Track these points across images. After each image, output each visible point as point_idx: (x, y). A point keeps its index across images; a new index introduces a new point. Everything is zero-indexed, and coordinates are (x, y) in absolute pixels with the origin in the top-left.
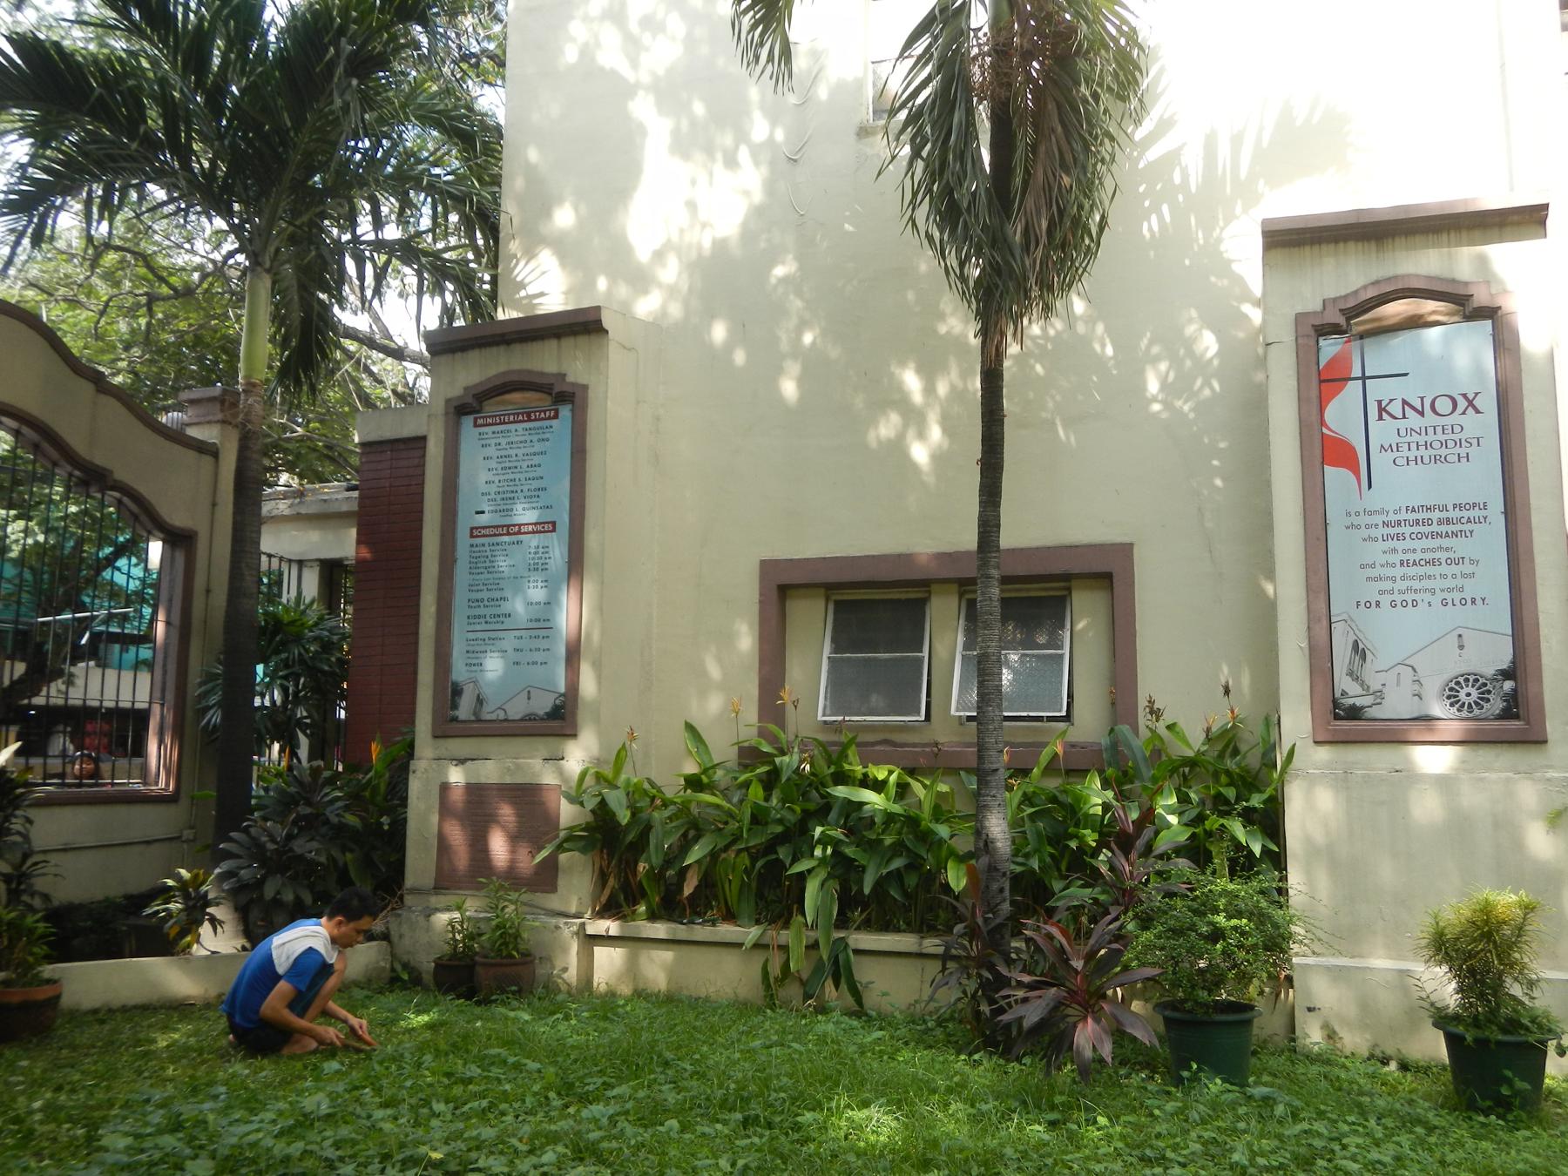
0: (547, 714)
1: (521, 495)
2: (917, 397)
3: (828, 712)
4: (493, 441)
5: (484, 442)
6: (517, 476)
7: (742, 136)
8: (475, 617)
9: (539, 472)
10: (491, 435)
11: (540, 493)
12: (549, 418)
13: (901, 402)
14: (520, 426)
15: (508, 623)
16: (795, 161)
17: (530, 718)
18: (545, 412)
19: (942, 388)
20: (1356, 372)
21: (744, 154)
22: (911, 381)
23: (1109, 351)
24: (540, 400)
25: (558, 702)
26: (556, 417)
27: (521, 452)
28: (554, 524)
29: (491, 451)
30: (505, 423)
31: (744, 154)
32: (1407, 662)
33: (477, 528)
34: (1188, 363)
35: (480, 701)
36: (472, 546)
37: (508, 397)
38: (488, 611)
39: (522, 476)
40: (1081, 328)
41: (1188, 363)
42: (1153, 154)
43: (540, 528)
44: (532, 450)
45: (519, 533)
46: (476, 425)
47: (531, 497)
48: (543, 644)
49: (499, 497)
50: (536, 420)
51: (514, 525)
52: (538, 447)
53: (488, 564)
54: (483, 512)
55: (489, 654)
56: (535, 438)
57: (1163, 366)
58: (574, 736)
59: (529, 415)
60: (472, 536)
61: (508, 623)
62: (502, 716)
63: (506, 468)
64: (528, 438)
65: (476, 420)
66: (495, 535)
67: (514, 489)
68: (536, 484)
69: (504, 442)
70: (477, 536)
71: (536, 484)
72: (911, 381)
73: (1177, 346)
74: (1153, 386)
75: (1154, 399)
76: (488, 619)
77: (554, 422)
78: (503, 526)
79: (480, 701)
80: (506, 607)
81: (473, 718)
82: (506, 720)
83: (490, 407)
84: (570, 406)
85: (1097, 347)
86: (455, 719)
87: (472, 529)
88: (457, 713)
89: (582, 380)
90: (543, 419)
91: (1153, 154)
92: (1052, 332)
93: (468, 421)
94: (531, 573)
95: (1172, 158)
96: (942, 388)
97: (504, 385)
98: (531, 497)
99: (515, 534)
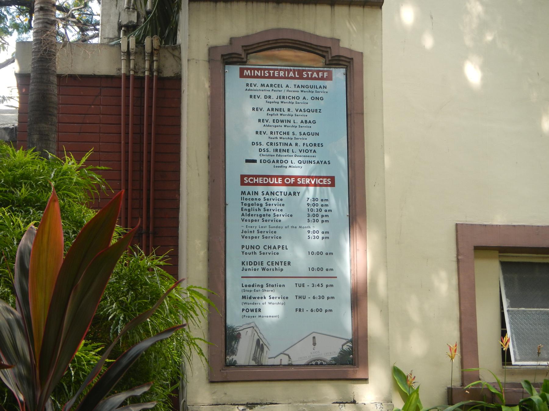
0: (334, 359)
1: (296, 149)
3: (518, 358)
4: (262, 94)
5: (253, 93)
6: (291, 130)
8: (250, 263)
9: (314, 128)
10: (259, 88)
11: (316, 148)
12: (322, 79)
14: (292, 83)
15: (287, 271)
17: (317, 363)
18: (313, 72)
24: (313, 60)
25: (345, 348)
26: (329, 78)
27: (293, 107)
28: (333, 179)
29: (261, 103)
30: (273, 77)
32: (286, 352)
33: (248, 176)
35: (260, 346)
36: (243, 193)
37: (276, 52)
38: (265, 259)
39: (297, 131)
43: (318, 181)
44: (307, 107)
45: (295, 184)
46: (242, 76)
47: (307, 151)
48: (327, 292)
49: (271, 148)
50: (307, 78)
51: (290, 177)
52: (312, 105)
53: (262, 212)
54: (254, 161)
55: (267, 300)
56: (308, 96)
58: (365, 380)
59: (300, 73)
60: (243, 183)
61: (287, 271)
62: (285, 361)
63: (278, 121)
64: (301, 95)
65: (242, 71)
66: (268, 184)
67: (289, 141)
68: (310, 140)
69: (274, 95)
70: (248, 184)
71: (310, 140)
76: (265, 265)
77: (327, 83)
78: (277, 177)
79: (260, 346)
80: (285, 255)
81: (253, 363)
82: (290, 365)
83: (255, 61)
84: (343, 70)
86: (233, 364)
87: (242, 177)
88: (234, 358)
89: (357, 47)
90: (315, 79)
93: (233, 71)
94: (311, 224)
97: (276, 41)
98: (307, 151)
99: (290, 185)
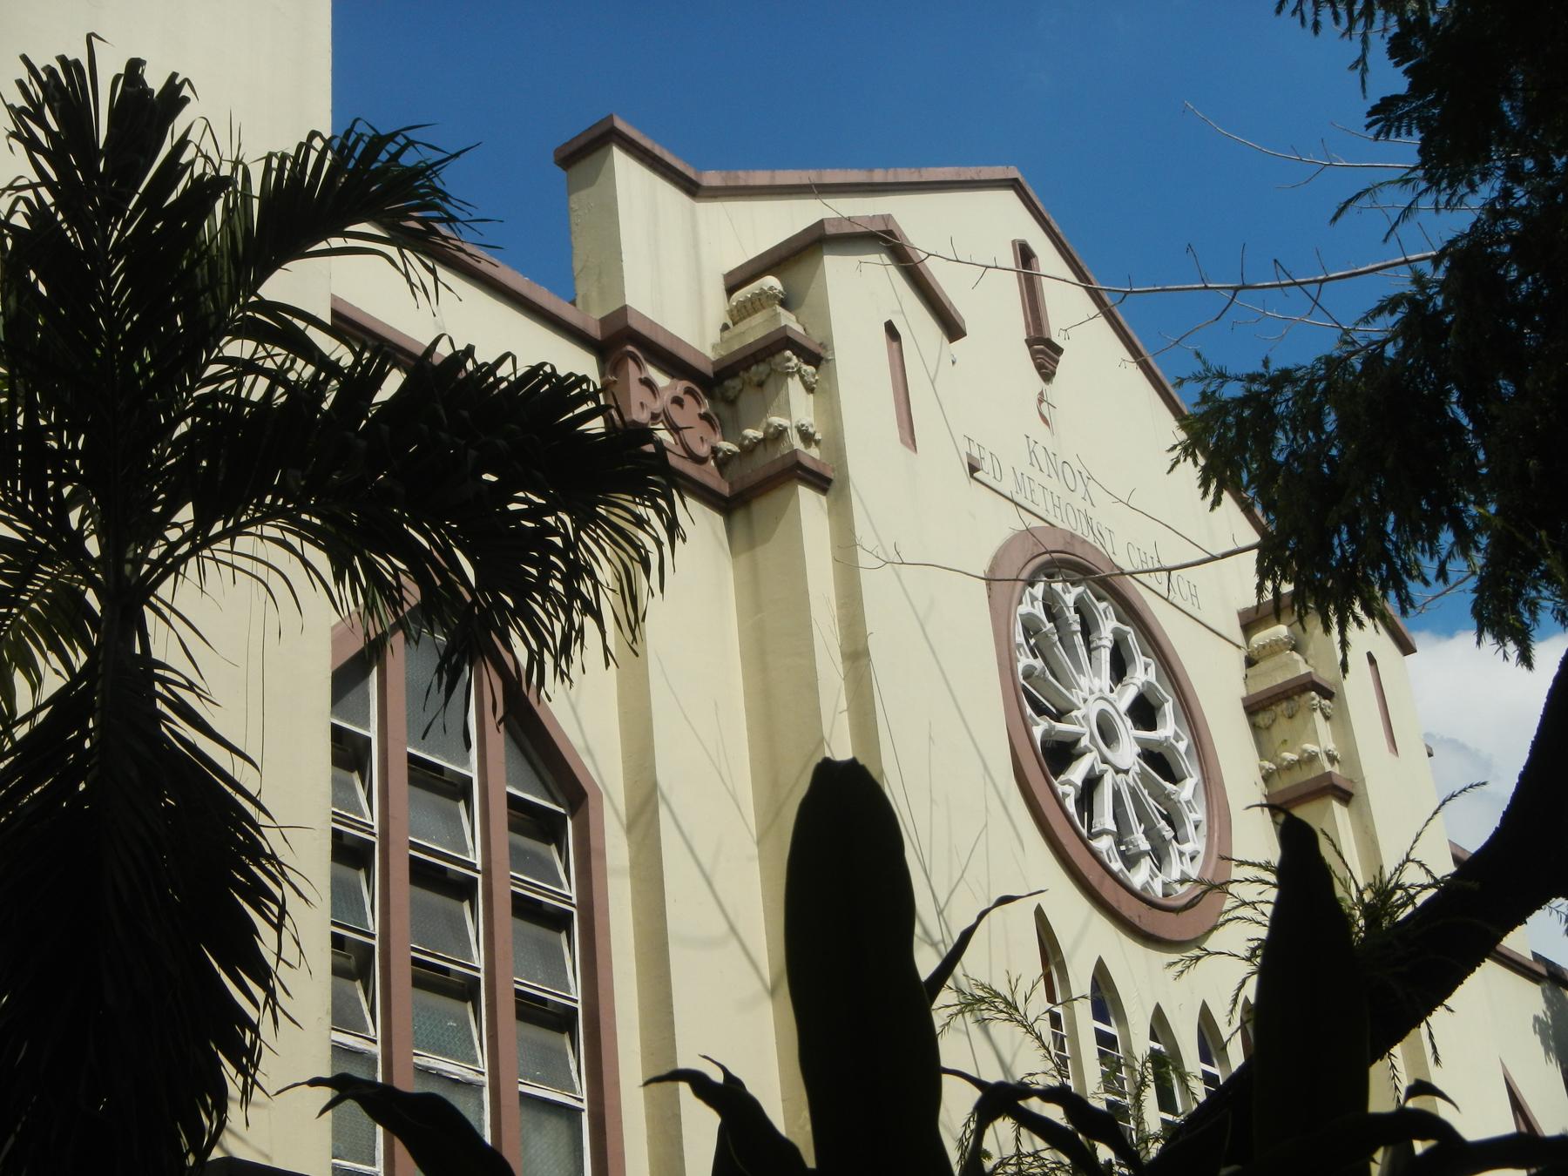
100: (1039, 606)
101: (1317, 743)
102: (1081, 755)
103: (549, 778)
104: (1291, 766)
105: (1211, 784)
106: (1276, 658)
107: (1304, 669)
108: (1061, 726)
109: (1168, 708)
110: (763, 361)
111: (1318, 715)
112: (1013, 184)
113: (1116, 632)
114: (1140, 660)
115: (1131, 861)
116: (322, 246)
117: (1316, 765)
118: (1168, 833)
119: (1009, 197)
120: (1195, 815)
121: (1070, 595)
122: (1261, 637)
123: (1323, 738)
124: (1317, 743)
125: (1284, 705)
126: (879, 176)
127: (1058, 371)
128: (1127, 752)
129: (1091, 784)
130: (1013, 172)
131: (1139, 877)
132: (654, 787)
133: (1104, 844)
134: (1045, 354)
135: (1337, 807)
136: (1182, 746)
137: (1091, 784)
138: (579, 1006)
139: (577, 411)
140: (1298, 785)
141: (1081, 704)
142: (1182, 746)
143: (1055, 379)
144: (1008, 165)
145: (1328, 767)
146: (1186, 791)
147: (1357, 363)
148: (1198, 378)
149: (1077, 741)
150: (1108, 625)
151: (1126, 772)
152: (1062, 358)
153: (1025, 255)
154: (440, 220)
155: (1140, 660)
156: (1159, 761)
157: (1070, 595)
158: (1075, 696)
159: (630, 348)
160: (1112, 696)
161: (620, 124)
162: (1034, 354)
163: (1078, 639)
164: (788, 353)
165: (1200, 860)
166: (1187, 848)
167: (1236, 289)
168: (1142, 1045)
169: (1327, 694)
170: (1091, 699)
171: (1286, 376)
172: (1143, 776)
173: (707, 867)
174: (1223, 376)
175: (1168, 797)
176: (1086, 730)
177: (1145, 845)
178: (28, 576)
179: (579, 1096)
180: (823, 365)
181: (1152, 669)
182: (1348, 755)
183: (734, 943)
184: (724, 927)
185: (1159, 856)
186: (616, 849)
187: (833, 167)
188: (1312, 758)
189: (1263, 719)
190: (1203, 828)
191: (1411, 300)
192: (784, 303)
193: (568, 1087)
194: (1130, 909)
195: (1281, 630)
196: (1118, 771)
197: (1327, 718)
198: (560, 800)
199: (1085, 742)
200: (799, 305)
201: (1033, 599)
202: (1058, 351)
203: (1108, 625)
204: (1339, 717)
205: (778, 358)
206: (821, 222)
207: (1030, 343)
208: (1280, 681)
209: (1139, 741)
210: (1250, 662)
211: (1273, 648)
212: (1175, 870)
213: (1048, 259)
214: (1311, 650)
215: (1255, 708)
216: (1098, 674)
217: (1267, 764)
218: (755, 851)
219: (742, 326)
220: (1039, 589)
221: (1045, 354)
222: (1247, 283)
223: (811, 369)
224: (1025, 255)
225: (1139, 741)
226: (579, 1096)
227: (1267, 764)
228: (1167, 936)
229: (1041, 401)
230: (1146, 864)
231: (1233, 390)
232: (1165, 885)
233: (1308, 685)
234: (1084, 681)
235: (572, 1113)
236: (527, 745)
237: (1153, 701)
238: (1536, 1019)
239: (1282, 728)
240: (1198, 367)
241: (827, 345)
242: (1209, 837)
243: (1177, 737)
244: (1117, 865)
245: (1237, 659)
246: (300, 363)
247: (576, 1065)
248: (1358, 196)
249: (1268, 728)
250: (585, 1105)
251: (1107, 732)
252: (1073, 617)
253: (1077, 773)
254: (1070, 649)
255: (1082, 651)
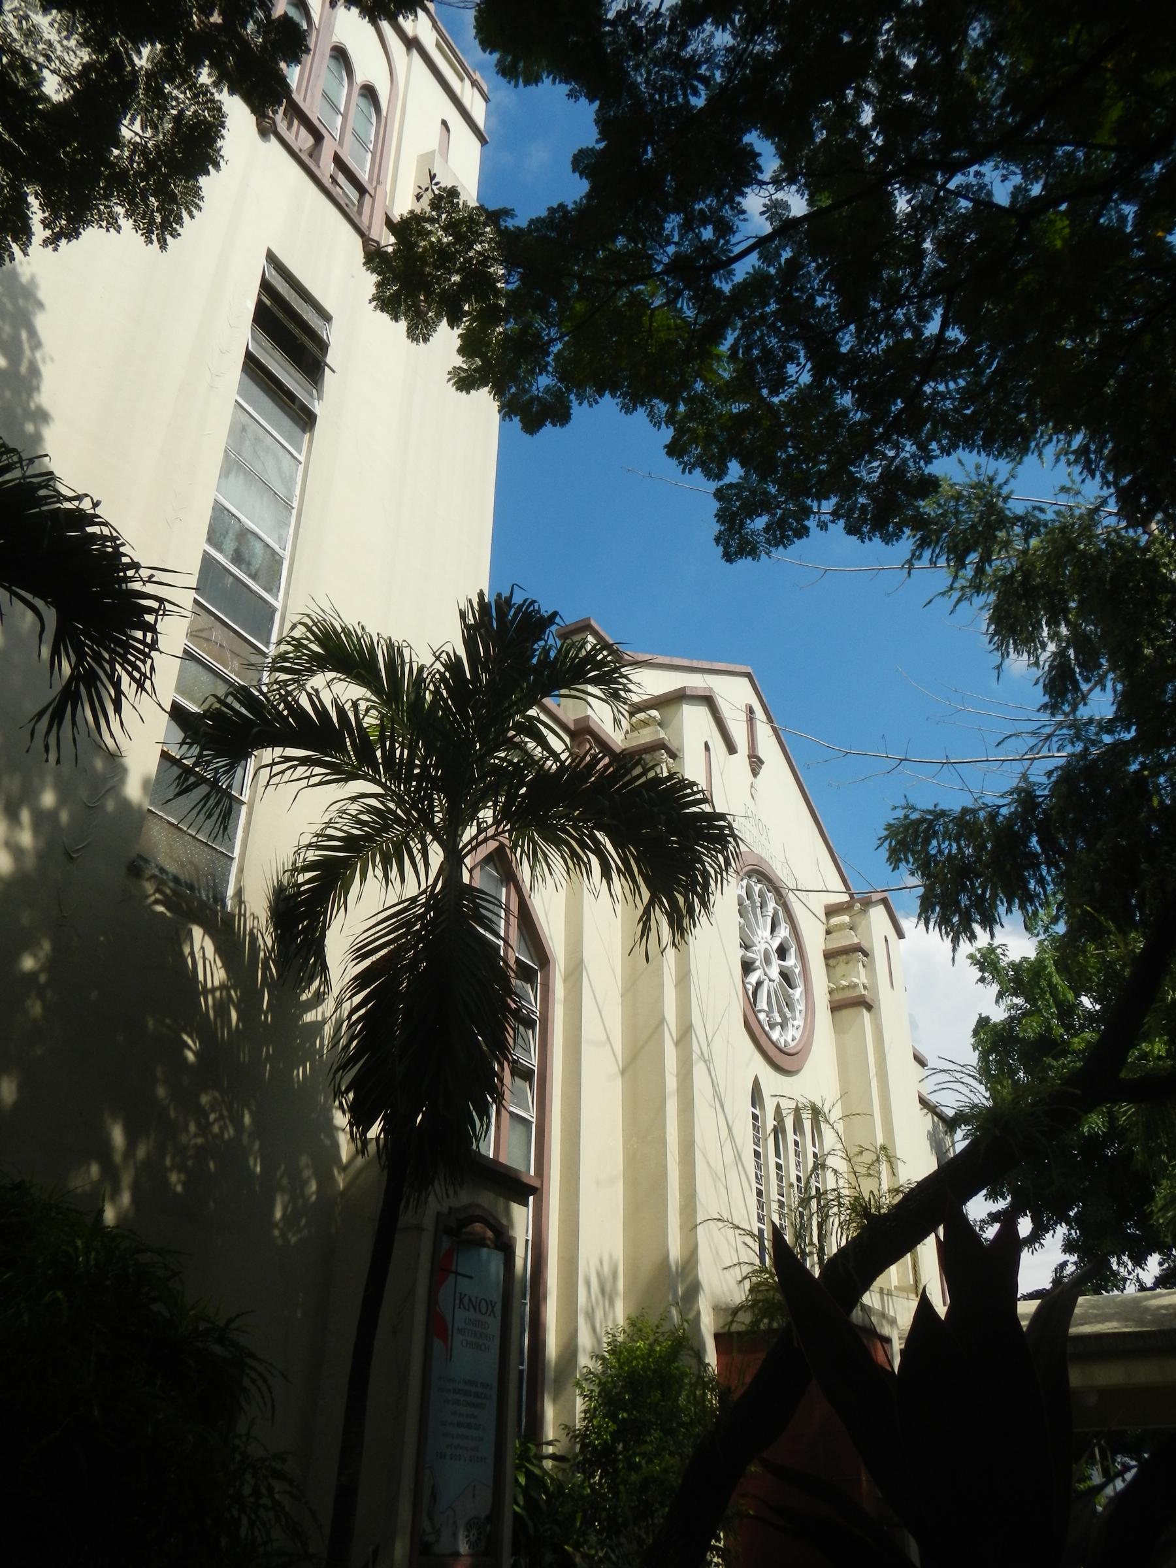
2: (118, 1158)
7: (28, 795)
13: (104, 1152)
16: (72, 858)
19: (141, 1152)
20: (454, 1269)
21: (25, 816)
22: (118, 1136)
23: (258, 1169)
31: (25, 816)
34: (300, 1202)
40: (245, 1139)
41: (300, 1202)
42: (309, 1017)
57: (286, 1198)
72: (118, 1136)
73: (298, 1185)
74: (278, 1214)
75: (276, 1225)
85: (251, 1162)
91: (309, 1017)
92: (226, 1136)
95: (318, 1026)
96: (141, 1152)
100: (744, 890)
101: (859, 979)
102: (755, 970)
103: (532, 949)
104: (844, 988)
105: (808, 991)
106: (842, 932)
107: (856, 940)
108: (749, 954)
109: (793, 950)
110: (649, 753)
111: (860, 964)
112: (748, 676)
113: (774, 909)
114: (783, 925)
115: (772, 1026)
116: (556, 693)
117: (857, 990)
118: (789, 1015)
119: (746, 681)
120: (800, 1007)
121: (757, 888)
122: (835, 920)
123: (861, 977)
124: (859, 979)
125: (844, 957)
126: (695, 664)
127: (762, 772)
128: (774, 972)
129: (759, 984)
130: (749, 670)
131: (775, 1034)
132: (582, 961)
133: (762, 1016)
134: (756, 763)
135: (865, 1011)
136: (797, 971)
137: (759, 984)
138: (536, 1069)
139: (636, 784)
140: (847, 998)
141: (757, 943)
142: (797, 971)
143: (759, 776)
144: (747, 665)
145: (863, 992)
146: (797, 993)
147: (982, 814)
148: (903, 808)
149: (753, 963)
150: (771, 905)
151: (773, 981)
152: (763, 766)
153: (751, 710)
154: (621, 689)
155: (783, 925)
156: (785, 976)
157: (757, 888)
158: (755, 939)
159: (588, 737)
160: (771, 942)
161: (593, 623)
162: (751, 763)
163: (758, 910)
164: (663, 751)
165: (801, 1029)
166: (796, 1023)
167: (902, 760)
168: (771, 1124)
169: (866, 954)
170: (762, 941)
171: (943, 813)
172: (780, 983)
173: (600, 1004)
174: (914, 809)
175: (789, 996)
176: (758, 957)
177: (779, 1020)
178: (386, 828)
179: (531, 1115)
180: (677, 759)
181: (788, 930)
182: (873, 986)
183: (608, 1046)
184: (605, 1037)
185: (783, 1026)
186: (559, 990)
187: (677, 657)
188: (856, 986)
189: (832, 962)
190: (803, 1013)
191: (1023, 790)
192: (659, 724)
193: (527, 1110)
194: (772, 1052)
195: (845, 919)
196: (771, 980)
197: (864, 966)
198: (537, 962)
199: (758, 963)
200: (668, 727)
201: (742, 887)
202: (762, 762)
203: (771, 905)
204: (870, 967)
205: (657, 753)
206: (684, 688)
207: (750, 757)
208: (843, 944)
209: (780, 966)
210: (828, 932)
211: (841, 927)
212: (791, 1033)
213: (759, 713)
214: (860, 930)
215: (829, 956)
216: (765, 930)
217: (832, 985)
218: (620, 1000)
219: (636, 734)
220: (745, 883)
221: (756, 763)
222: (908, 758)
223: (671, 761)
224: (751, 710)
225: (780, 966)
226: (531, 1115)
227: (832, 985)
228: (786, 1068)
229: (752, 787)
230: (778, 1028)
231: (915, 816)
232: (785, 1041)
233: (858, 948)
234: (759, 932)
235: (525, 1122)
236: (525, 932)
237: (785, 946)
238: (929, 1132)
239: (841, 969)
240: (903, 803)
241: (681, 749)
242: (806, 1019)
243: (796, 966)
244: (767, 1028)
245: (822, 929)
246: (539, 749)
247: (531, 1098)
248: (1011, 736)
249: (834, 967)
250: (534, 1120)
251: (767, 960)
252: (758, 900)
253: (753, 978)
254: (755, 914)
255: (759, 916)
